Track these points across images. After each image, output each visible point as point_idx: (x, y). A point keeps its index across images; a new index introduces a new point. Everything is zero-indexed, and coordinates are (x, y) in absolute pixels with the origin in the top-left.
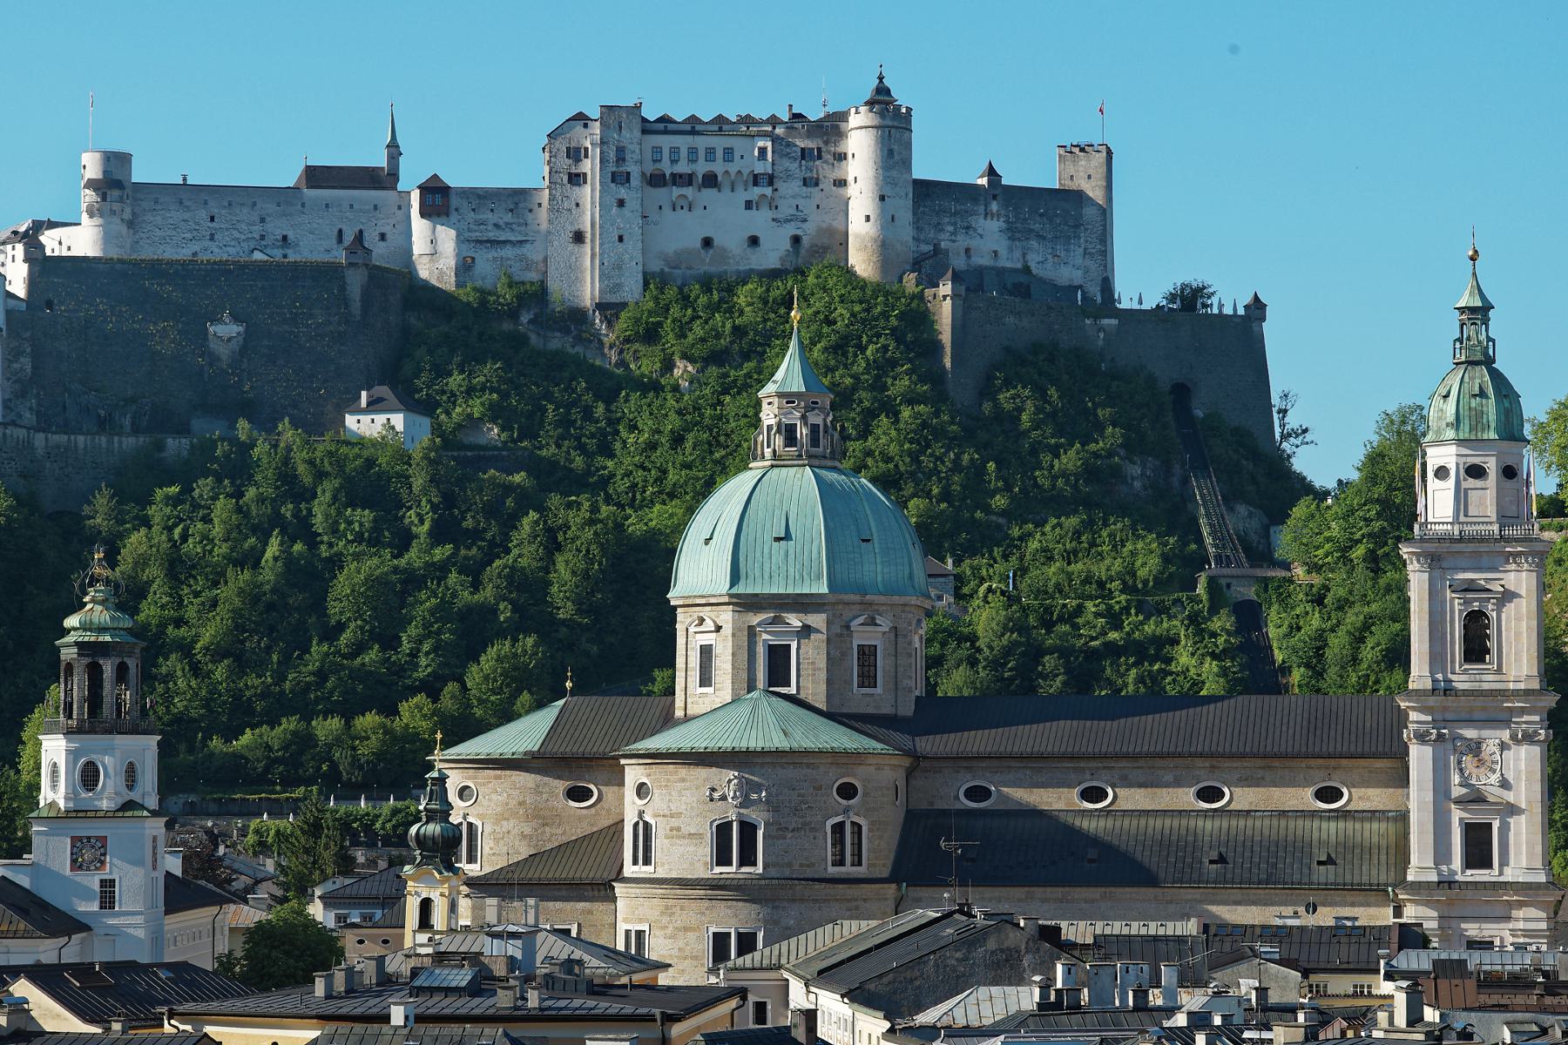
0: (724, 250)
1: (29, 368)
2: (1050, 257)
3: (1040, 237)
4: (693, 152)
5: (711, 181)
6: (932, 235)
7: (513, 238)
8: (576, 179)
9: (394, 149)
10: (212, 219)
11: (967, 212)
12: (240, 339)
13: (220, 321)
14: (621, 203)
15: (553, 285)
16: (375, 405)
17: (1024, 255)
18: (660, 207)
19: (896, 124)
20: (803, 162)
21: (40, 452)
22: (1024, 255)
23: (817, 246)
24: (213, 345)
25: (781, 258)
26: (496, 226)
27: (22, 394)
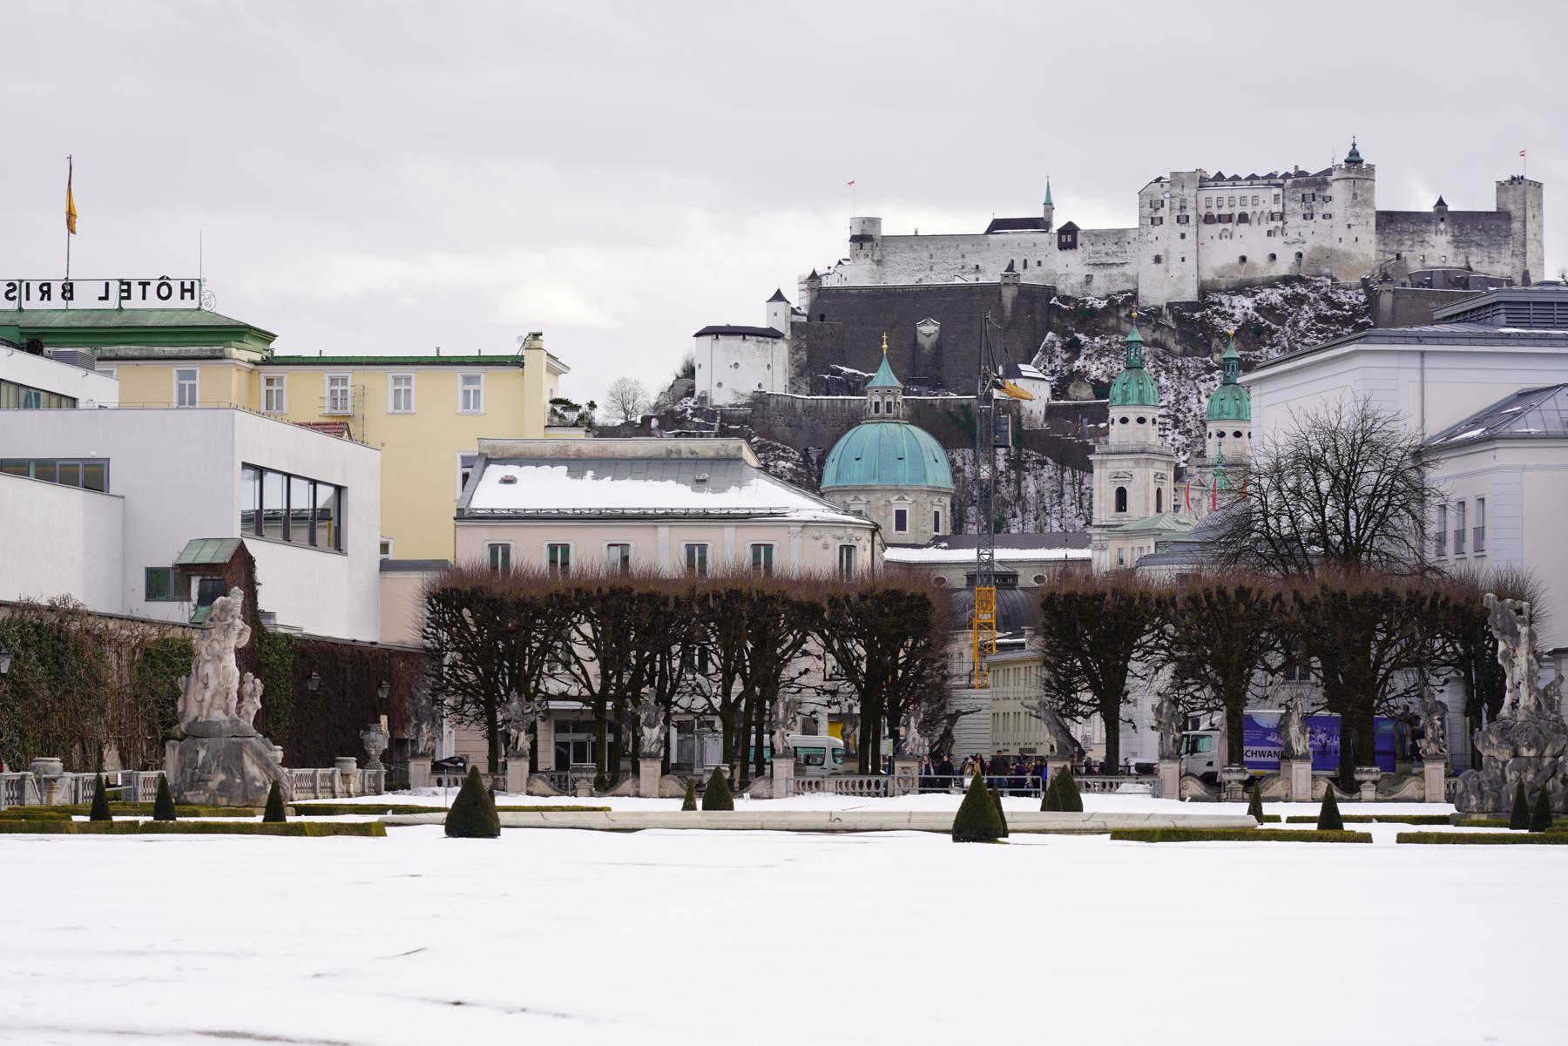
0: (1254, 264)
1: (805, 358)
2: (1486, 258)
3: (1479, 245)
5: (1243, 218)
6: (1395, 248)
7: (1117, 262)
9: (1049, 205)
12: (937, 335)
14: (1183, 236)
15: (1141, 292)
21: (799, 410)
24: (921, 339)
27: (800, 374)
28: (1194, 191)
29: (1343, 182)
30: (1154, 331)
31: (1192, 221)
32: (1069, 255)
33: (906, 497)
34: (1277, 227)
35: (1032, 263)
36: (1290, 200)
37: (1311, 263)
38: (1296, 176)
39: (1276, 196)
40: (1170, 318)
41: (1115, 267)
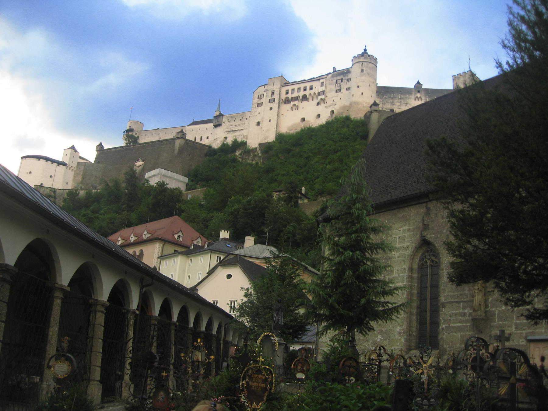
0: (308, 121)
1: (80, 179)
5: (305, 98)
7: (240, 129)
11: (406, 98)
12: (142, 166)
13: (138, 161)
14: (271, 109)
18: (288, 110)
19: (365, 60)
20: (336, 85)
23: (339, 113)
26: (236, 126)
28: (279, 86)
29: (356, 64)
30: (252, 161)
31: (277, 101)
32: (219, 129)
34: (321, 99)
35: (204, 138)
36: (330, 84)
38: (334, 72)
39: (322, 83)
40: (259, 152)
41: (238, 131)
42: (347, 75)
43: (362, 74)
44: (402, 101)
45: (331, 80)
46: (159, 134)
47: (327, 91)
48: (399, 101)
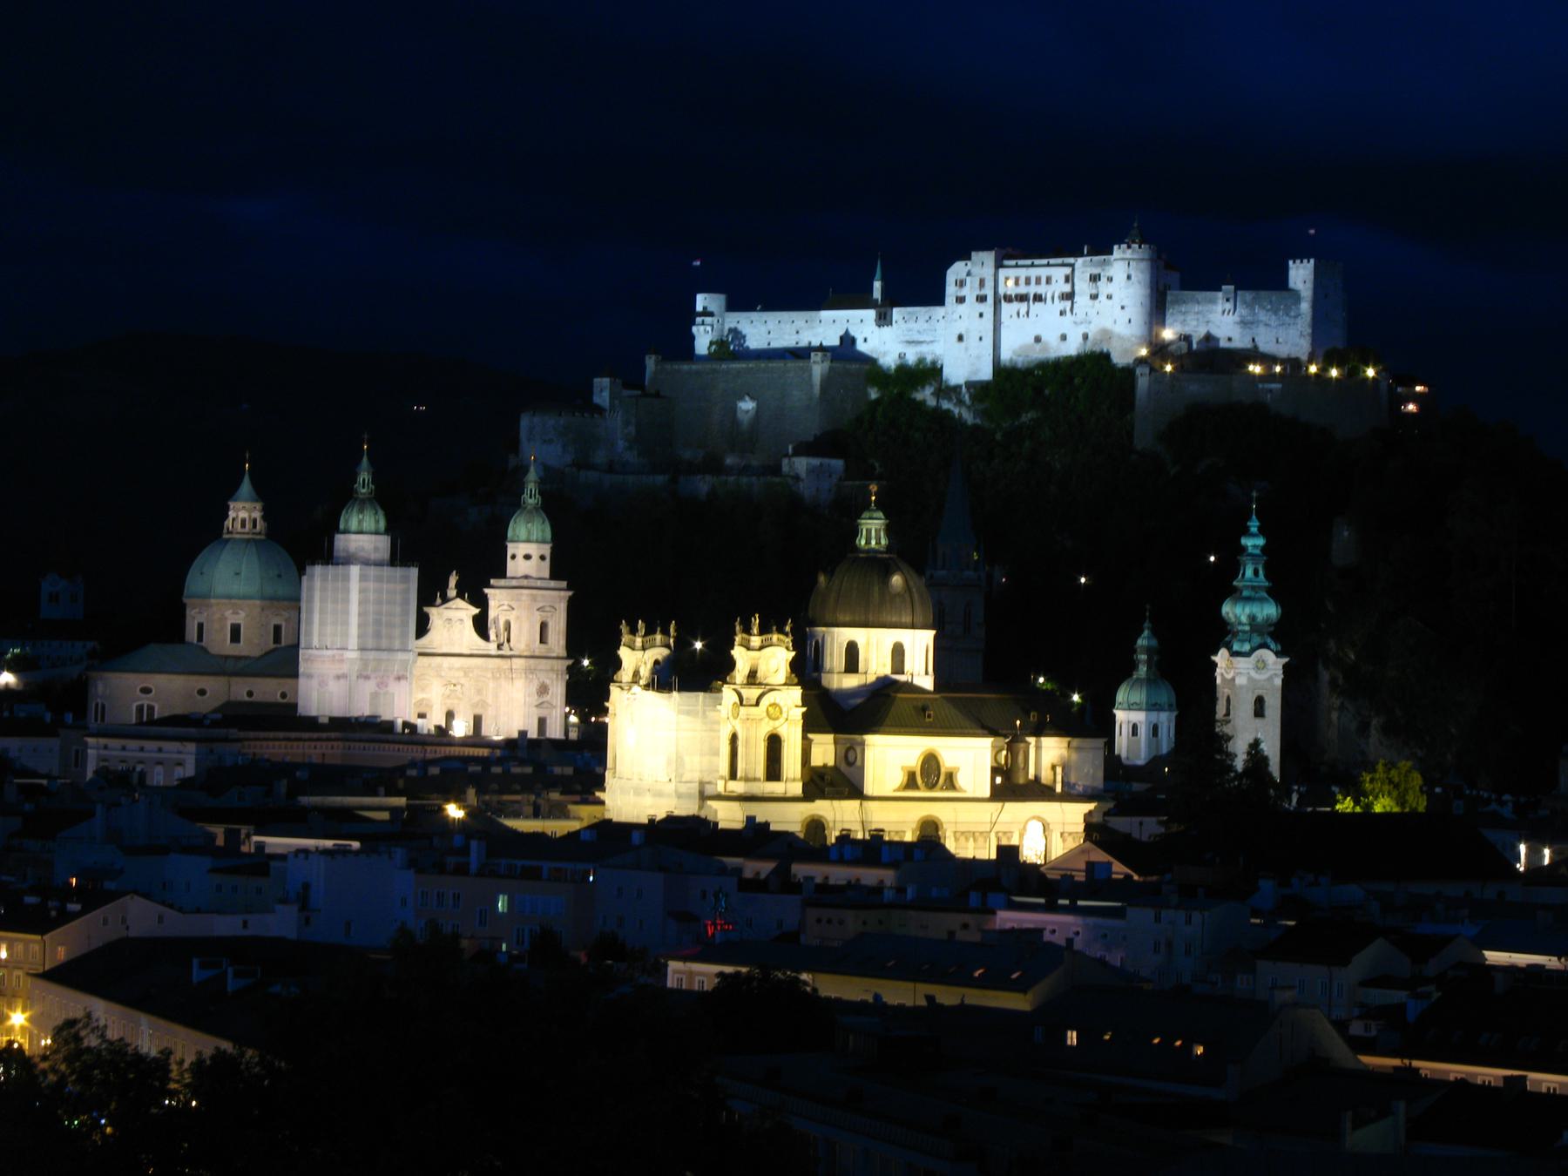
3: (1267, 325)
4: (1028, 281)
5: (1038, 298)
7: (928, 339)
8: (961, 300)
10: (769, 333)
12: (754, 411)
13: (742, 399)
14: (981, 315)
16: (797, 453)
17: (1253, 340)
19: (1135, 257)
22: (1253, 340)
24: (739, 415)
25: (1078, 349)
26: (919, 332)
28: (992, 271)
33: (240, 612)
37: (1095, 344)
40: (967, 397)
41: (924, 345)
42: (1107, 268)
43: (1131, 282)
44: (1200, 316)
45: (1081, 270)
46: (766, 322)
47: (1076, 291)
48: (1196, 317)
